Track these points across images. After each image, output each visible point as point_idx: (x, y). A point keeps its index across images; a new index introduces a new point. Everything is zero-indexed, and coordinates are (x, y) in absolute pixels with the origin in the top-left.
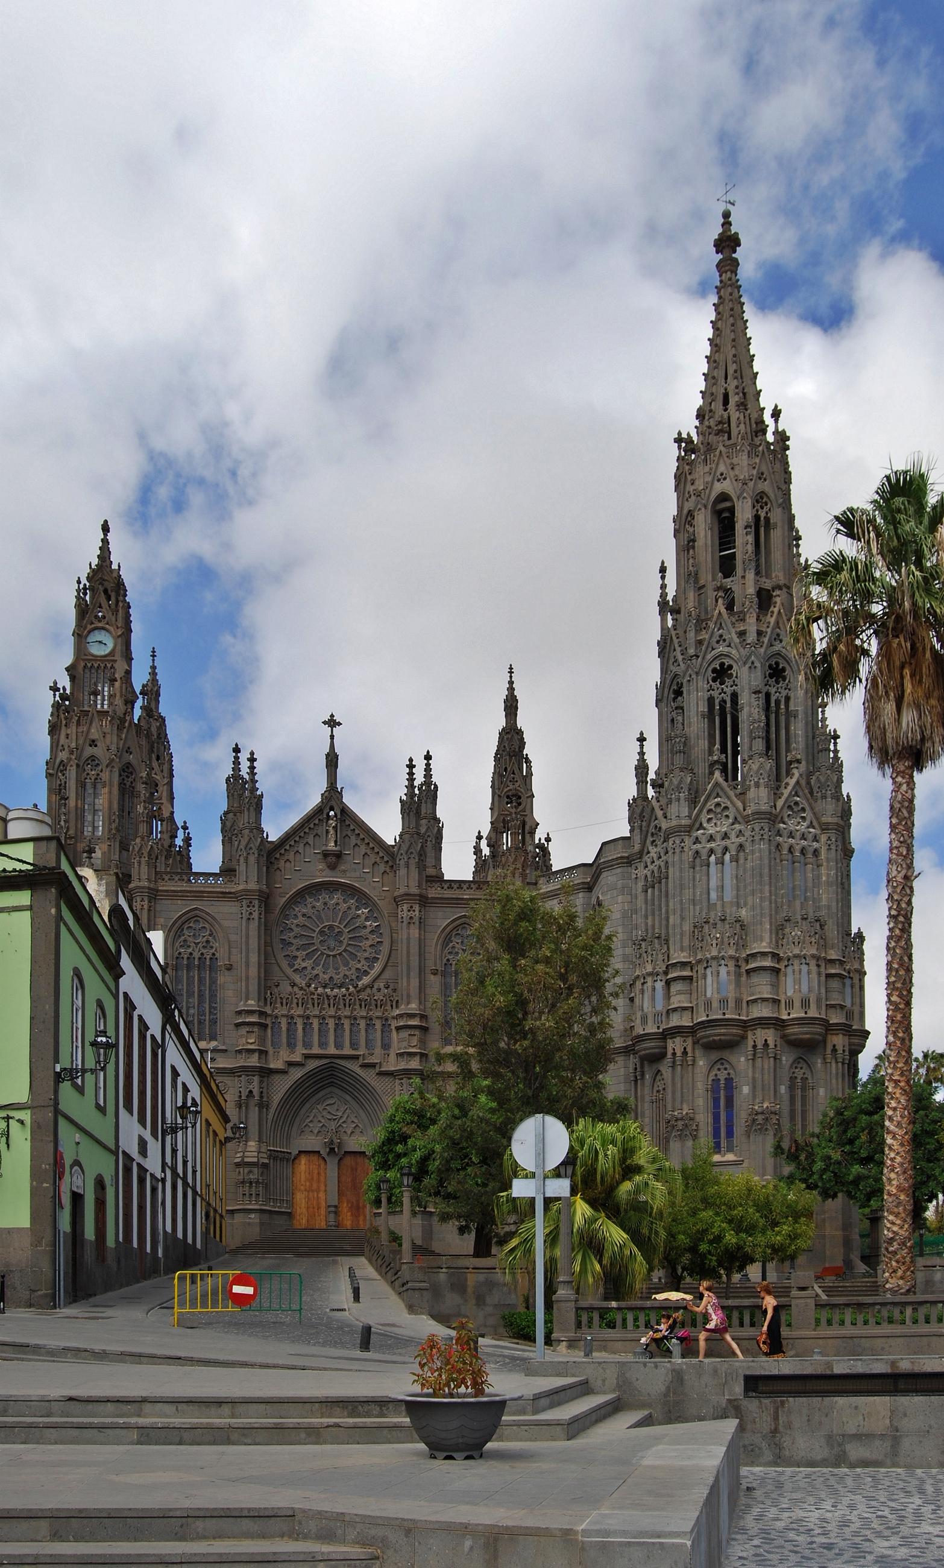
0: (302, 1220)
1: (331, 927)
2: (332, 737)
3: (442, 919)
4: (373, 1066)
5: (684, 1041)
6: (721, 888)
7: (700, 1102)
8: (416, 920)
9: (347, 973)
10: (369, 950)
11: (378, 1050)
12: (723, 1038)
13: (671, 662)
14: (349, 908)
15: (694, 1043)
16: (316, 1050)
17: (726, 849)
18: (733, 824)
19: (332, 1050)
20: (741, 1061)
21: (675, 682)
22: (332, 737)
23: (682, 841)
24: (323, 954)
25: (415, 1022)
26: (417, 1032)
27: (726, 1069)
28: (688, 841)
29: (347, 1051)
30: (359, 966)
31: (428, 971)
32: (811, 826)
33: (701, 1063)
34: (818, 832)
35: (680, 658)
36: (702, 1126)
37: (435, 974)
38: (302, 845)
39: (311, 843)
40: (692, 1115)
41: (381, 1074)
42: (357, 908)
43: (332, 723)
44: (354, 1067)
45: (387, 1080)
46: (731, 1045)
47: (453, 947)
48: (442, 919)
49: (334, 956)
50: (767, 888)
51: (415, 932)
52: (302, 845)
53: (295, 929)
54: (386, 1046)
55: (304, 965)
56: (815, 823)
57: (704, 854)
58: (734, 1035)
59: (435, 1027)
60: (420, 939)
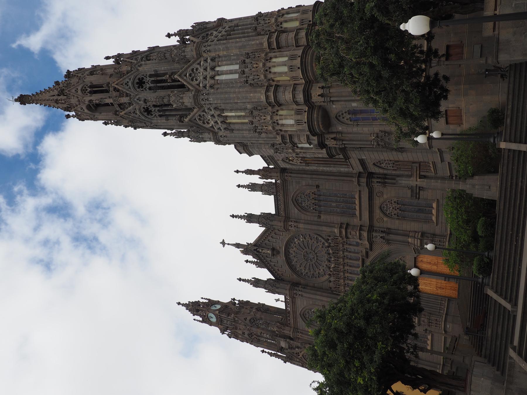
0: (453, 294)
1: (304, 256)
2: (228, 244)
3: (294, 211)
4: (367, 253)
5: (328, 139)
6: (239, 117)
7: (366, 129)
9: (324, 252)
10: (313, 241)
12: (320, 123)
14: (295, 247)
15: (329, 133)
17: (219, 115)
18: (206, 112)
20: (335, 108)
22: (228, 244)
23: (221, 136)
24: (316, 261)
27: (342, 114)
28: (221, 133)
29: (360, 263)
30: (321, 246)
31: (319, 220)
32: (199, 64)
33: (340, 128)
34: (202, 59)
36: (382, 128)
37: (320, 217)
38: (271, 263)
39: (270, 259)
40: (375, 135)
41: (371, 249)
42: (295, 243)
43: (223, 243)
44: (368, 263)
45: (374, 247)
46: (326, 115)
47: (307, 206)
48: (294, 211)
49: (317, 256)
50: (231, 96)
51: (301, 226)
52: (271, 263)
53: (306, 271)
54: (357, 245)
55: (322, 270)
56: (198, 62)
57: (225, 126)
58: (318, 115)
59: (345, 220)
60: (304, 223)
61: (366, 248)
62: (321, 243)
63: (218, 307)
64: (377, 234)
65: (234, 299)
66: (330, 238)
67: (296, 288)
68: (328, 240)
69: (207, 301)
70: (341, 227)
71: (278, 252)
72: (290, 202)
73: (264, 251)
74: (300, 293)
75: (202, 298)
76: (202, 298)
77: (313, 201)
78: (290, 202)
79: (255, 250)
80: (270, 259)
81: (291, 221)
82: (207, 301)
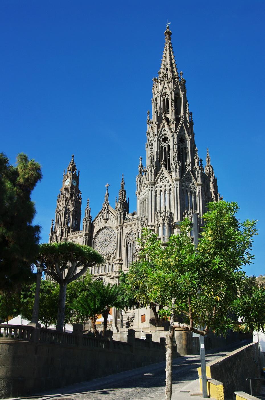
8: (119, 233)
11: (110, 272)
13: (150, 137)
16: (97, 274)
19: (100, 273)
21: (151, 143)
25: (118, 262)
26: (118, 265)
29: (104, 273)
30: (111, 248)
35: (152, 135)
37: (125, 247)
61: (111, 276)
62: (113, 248)
63: (75, 184)
64: (118, 281)
65: (81, 194)
66: (114, 254)
67: (87, 237)
68: (114, 253)
69: (77, 175)
70: (120, 260)
71: (106, 223)
72: (130, 228)
73: (105, 213)
74: (85, 240)
75: (79, 171)
76: (79, 171)
77: (132, 242)
78: (130, 228)
79: (105, 207)
80: (102, 218)
81: (121, 230)
82: (77, 175)
